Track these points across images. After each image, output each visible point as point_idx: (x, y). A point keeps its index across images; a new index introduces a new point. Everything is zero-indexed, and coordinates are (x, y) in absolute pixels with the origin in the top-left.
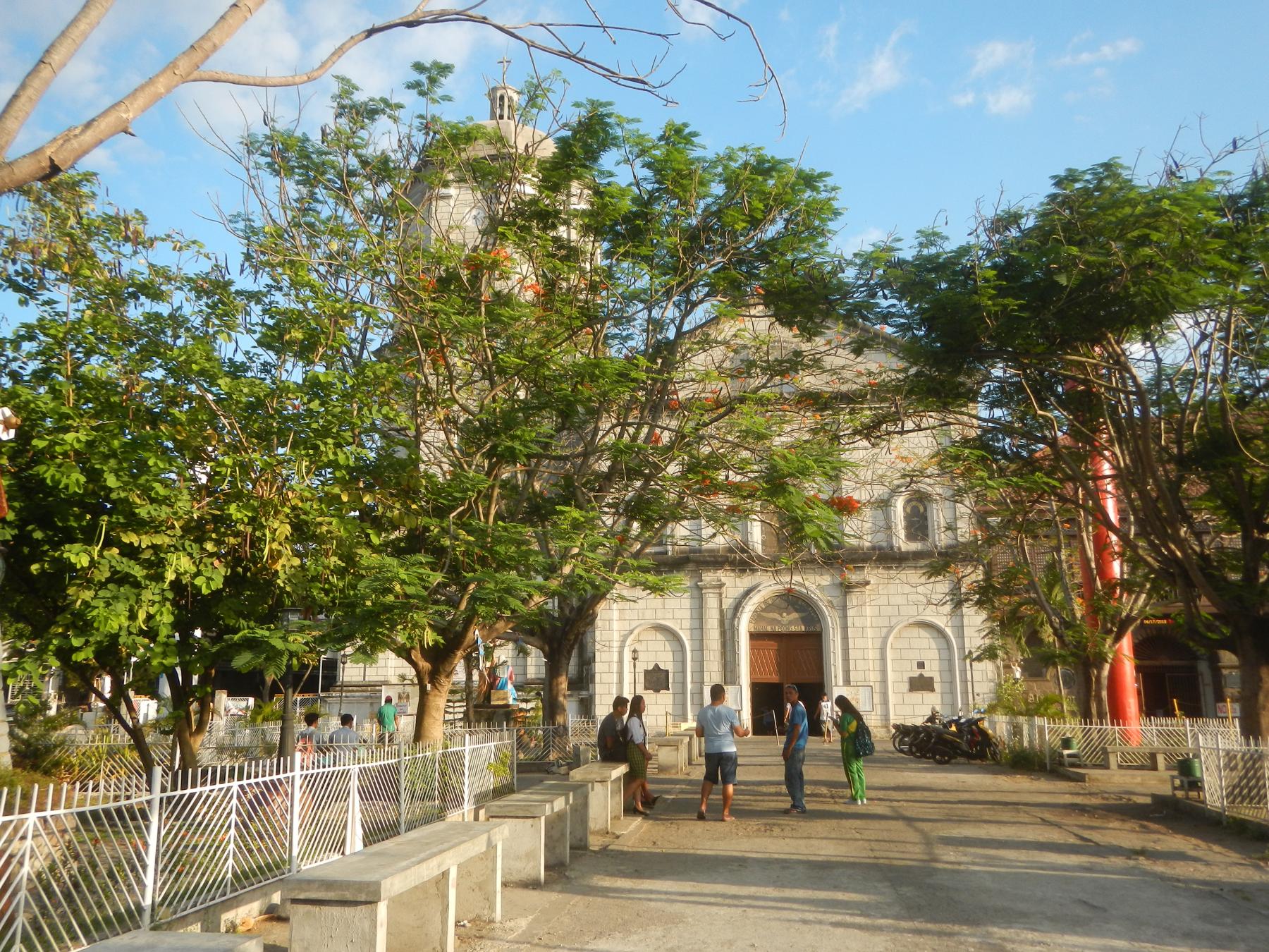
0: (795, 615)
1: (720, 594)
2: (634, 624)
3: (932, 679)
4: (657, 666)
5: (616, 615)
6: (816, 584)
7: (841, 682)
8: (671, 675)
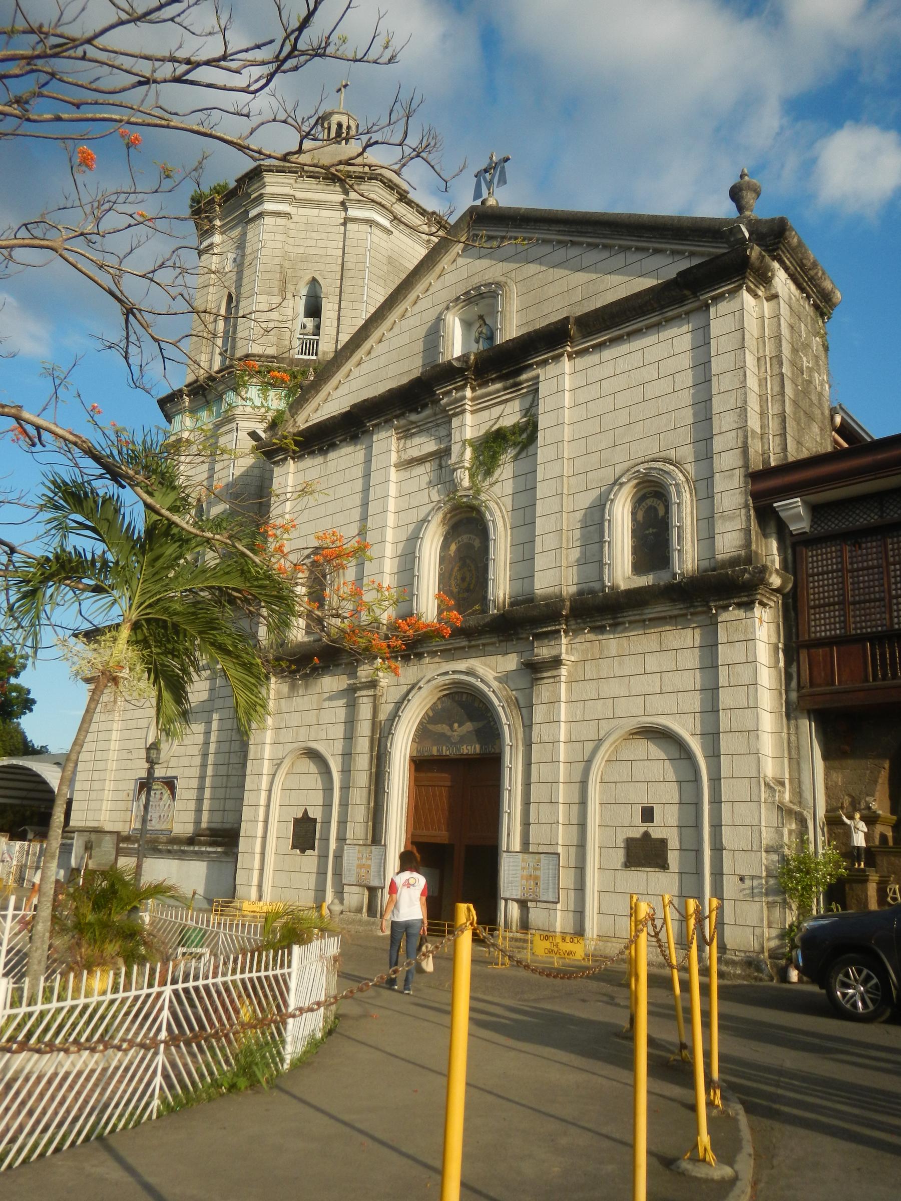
0: (469, 726)
3: (663, 842)
4: (306, 812)
5: (269, 736)
6: (490, 671)
7: (517, 846)
8: (318, 826)
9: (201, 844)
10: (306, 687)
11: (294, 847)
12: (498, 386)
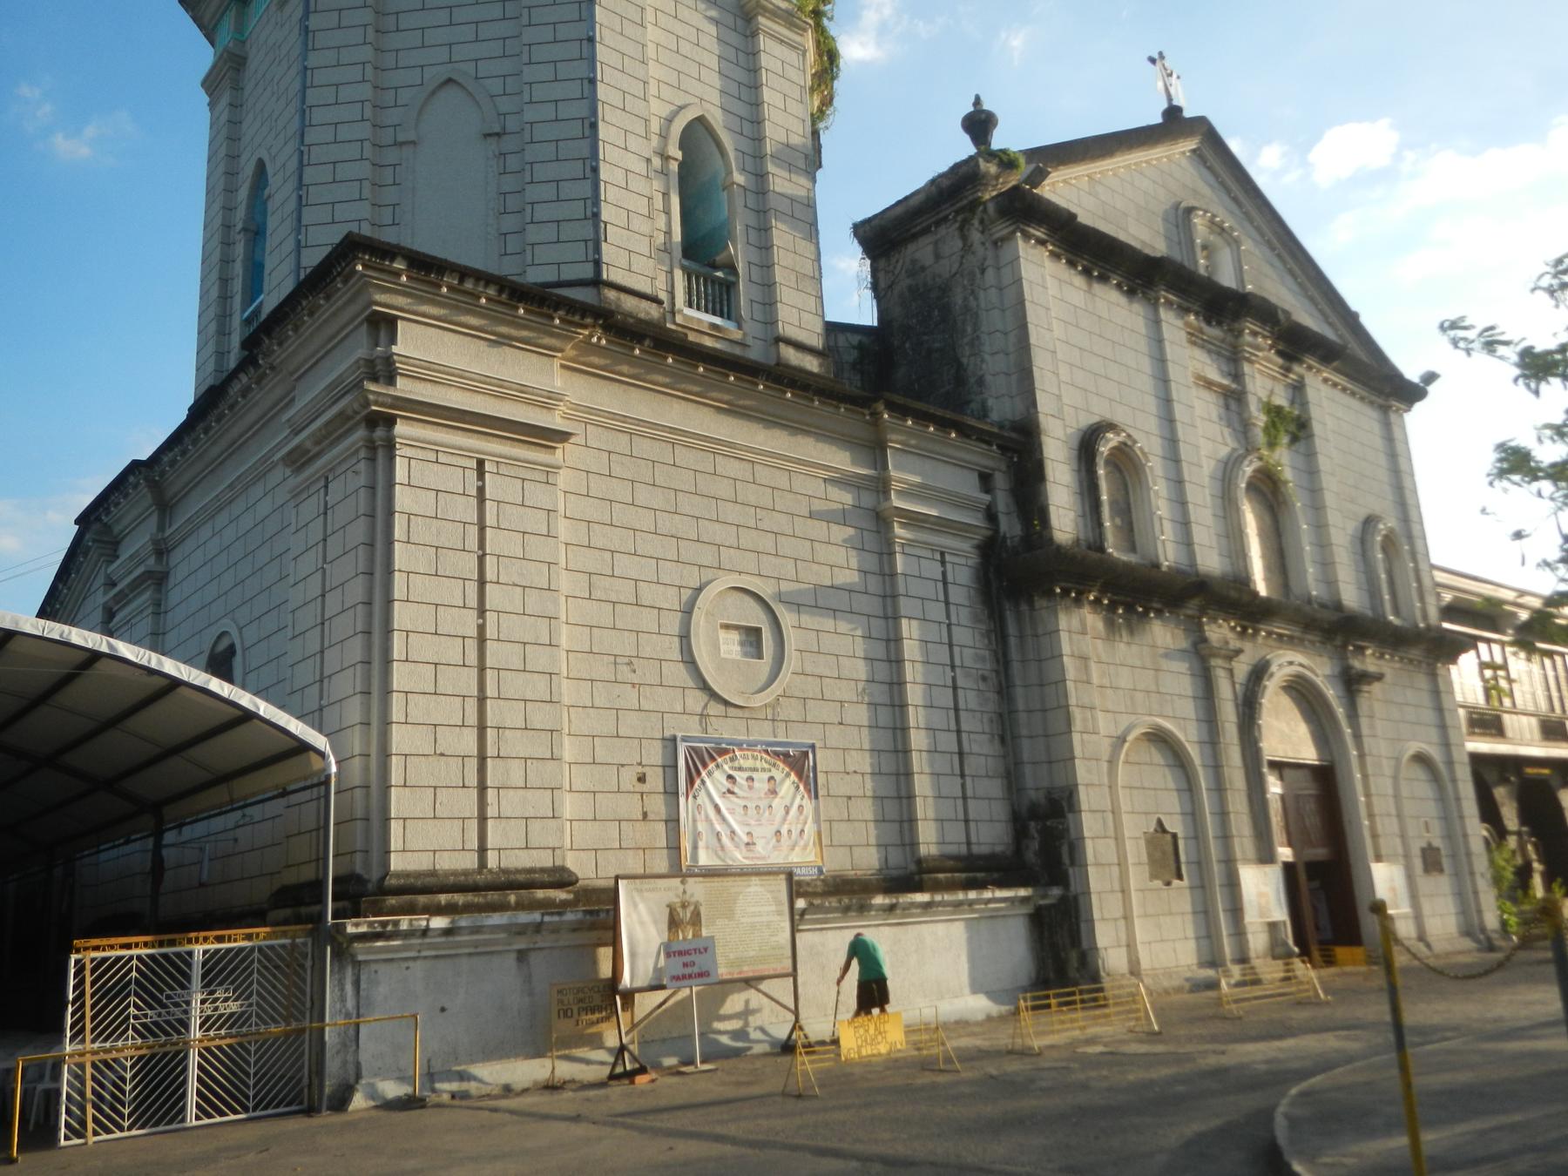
1: (1231, 672)
2: (1125, 721)
4: (1160, 823)
8: (1181, 843)
9: (936, 887)
10: (1131, 632)
11: (1153, 876)
12: (1280, 361)
